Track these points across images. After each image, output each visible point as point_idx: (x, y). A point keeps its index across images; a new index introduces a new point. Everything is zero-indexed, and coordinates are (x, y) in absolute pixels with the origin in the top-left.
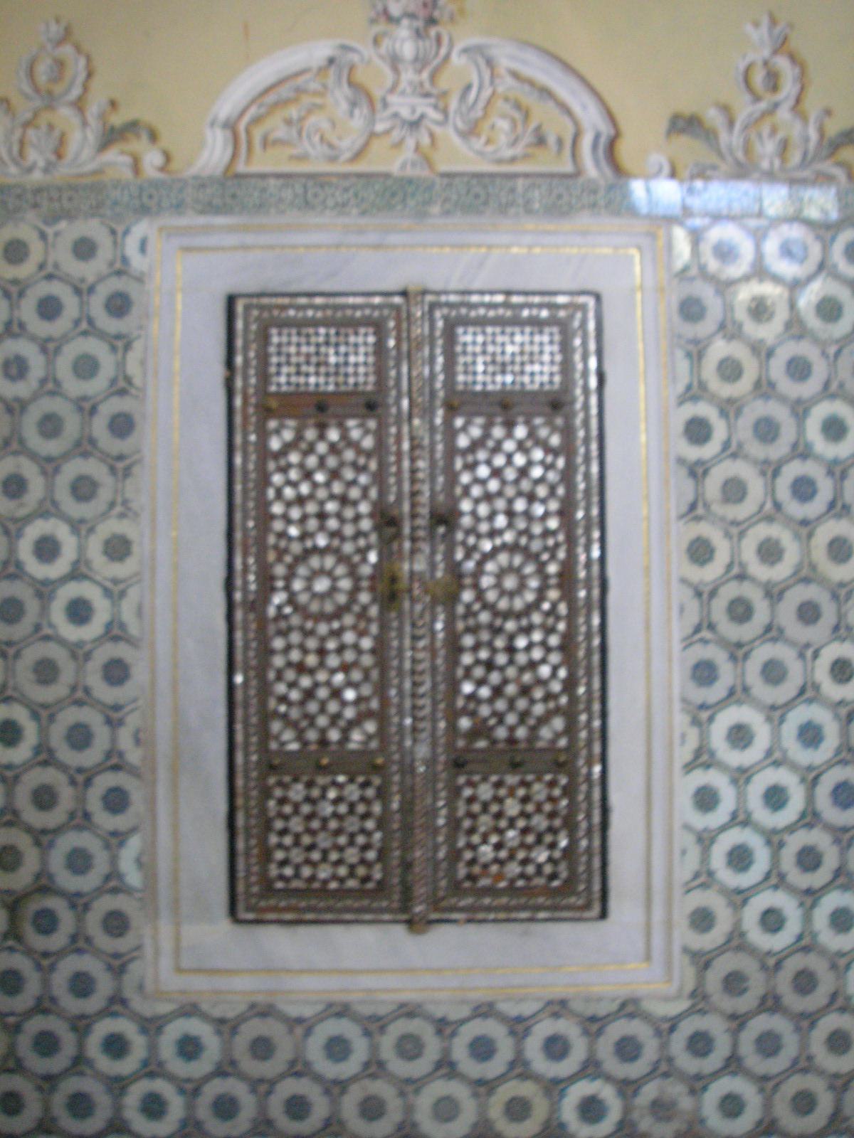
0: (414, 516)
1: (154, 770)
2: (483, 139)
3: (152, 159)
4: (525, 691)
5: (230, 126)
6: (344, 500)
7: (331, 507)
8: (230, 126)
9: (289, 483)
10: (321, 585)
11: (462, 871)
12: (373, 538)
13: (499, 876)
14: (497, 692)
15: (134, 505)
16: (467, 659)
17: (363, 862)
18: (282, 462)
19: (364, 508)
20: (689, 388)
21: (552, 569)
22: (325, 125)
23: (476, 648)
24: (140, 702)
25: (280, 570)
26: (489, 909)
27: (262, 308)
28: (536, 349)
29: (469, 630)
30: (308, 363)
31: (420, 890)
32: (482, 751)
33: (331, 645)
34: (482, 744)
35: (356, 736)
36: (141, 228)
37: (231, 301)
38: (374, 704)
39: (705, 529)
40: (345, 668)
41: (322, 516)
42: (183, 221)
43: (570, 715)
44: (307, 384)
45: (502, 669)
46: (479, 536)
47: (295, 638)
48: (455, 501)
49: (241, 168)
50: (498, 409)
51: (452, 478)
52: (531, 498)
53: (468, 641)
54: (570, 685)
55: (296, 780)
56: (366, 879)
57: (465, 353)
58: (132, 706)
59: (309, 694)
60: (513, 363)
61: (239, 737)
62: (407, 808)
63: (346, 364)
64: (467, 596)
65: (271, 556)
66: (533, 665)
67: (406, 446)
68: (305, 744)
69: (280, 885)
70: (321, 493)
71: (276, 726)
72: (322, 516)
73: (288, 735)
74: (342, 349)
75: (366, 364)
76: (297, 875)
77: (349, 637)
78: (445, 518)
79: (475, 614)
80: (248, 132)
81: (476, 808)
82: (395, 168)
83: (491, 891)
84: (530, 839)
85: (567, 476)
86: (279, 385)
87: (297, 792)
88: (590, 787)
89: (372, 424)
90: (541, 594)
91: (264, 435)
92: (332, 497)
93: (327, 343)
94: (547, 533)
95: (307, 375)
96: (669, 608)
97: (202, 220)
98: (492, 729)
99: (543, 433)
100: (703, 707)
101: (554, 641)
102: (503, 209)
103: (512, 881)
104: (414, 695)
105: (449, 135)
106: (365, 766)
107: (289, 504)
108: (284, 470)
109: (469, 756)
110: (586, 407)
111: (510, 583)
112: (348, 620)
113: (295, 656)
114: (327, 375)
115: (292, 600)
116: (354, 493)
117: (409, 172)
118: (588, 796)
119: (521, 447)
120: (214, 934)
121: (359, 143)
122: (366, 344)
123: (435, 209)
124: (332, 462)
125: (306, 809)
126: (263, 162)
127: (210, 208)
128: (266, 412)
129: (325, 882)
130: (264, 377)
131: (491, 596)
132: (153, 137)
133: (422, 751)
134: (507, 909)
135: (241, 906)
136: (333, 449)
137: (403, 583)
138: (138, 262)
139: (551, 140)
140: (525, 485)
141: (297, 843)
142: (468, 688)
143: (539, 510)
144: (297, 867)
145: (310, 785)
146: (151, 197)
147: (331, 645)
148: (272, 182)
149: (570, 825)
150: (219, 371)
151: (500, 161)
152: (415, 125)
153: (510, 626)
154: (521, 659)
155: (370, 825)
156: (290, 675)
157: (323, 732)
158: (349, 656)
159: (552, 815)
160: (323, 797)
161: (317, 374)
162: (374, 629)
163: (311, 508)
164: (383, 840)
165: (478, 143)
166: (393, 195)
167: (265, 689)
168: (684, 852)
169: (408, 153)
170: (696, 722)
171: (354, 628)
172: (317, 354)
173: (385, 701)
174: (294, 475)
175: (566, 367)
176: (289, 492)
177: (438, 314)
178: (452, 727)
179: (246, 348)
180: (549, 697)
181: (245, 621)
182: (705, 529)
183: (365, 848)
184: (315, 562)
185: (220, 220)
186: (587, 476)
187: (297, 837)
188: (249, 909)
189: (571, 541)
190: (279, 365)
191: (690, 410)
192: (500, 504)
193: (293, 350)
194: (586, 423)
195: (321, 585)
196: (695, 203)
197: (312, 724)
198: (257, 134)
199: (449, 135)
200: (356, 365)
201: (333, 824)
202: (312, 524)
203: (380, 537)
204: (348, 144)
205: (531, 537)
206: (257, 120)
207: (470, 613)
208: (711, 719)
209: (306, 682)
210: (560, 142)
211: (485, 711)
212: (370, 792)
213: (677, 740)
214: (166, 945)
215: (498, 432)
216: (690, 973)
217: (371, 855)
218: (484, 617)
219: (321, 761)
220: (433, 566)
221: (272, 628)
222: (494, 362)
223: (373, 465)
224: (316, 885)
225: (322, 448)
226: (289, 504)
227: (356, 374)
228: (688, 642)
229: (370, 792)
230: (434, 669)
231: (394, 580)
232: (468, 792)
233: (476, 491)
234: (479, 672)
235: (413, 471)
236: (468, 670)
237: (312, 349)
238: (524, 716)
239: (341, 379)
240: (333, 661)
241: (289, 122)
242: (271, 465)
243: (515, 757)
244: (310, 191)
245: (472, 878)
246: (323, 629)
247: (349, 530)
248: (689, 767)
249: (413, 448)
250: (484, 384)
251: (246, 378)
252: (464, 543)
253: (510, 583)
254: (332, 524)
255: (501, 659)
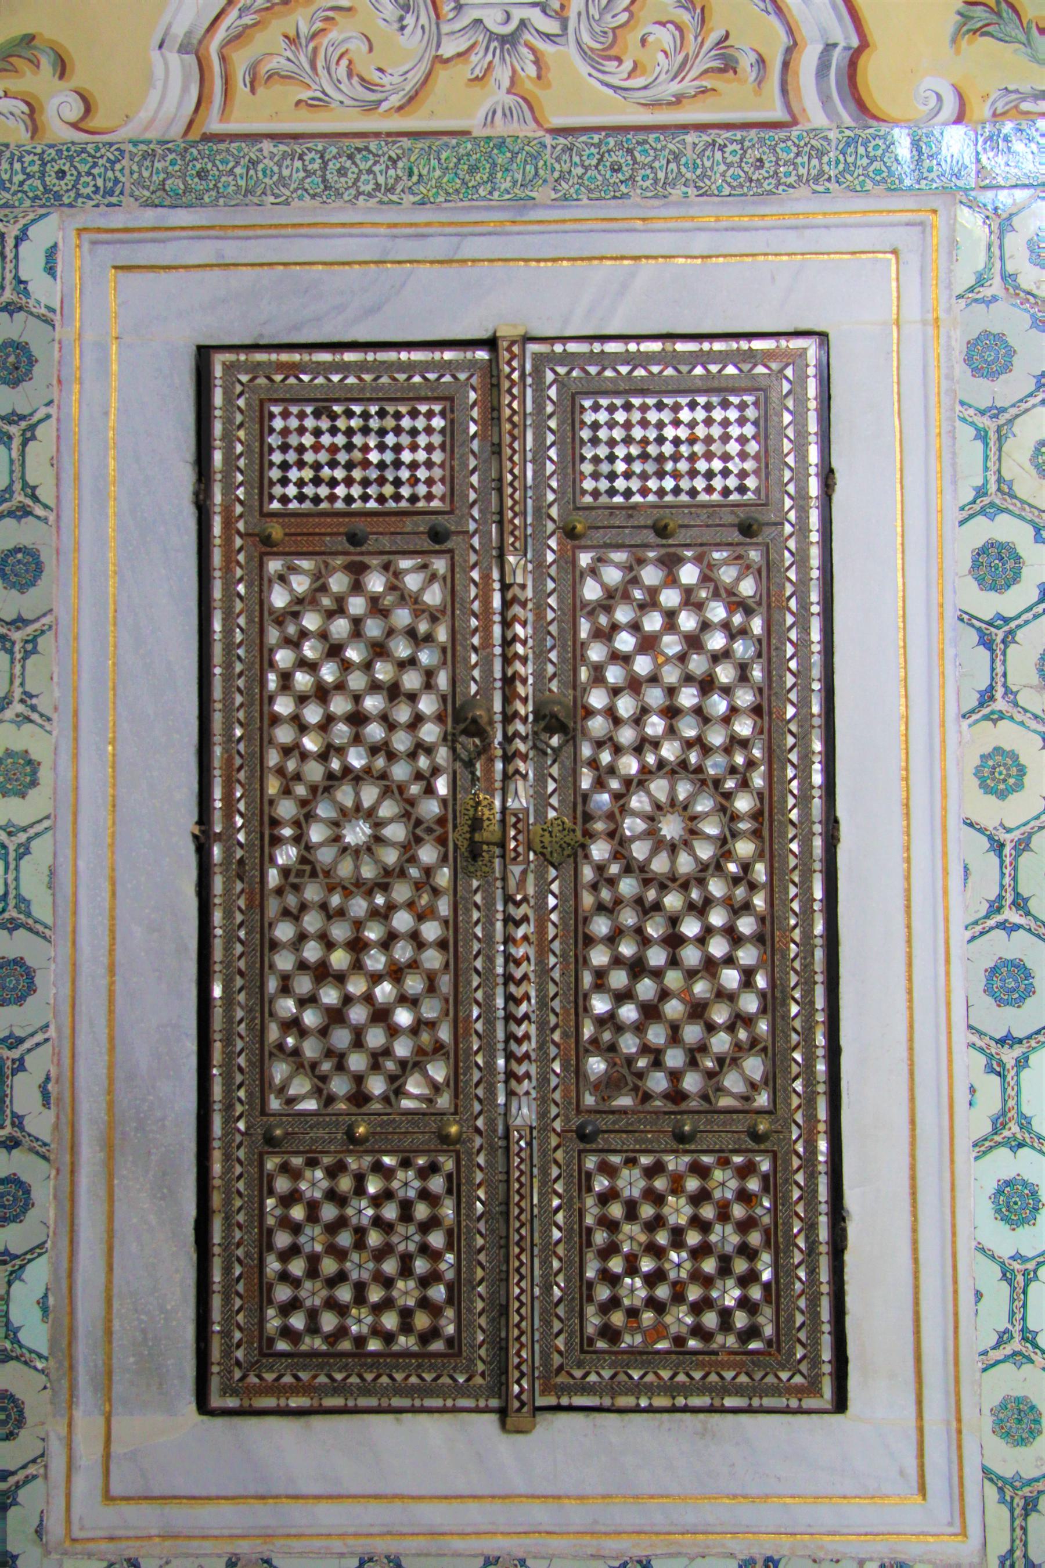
0: (508, 718)
1: (74, 1148)
2: (628, 65)
3: (61, 107)
4: (698, 1011)
5: (194, 49)
6: (394, 692)
7: (372, 703)
8: (194, 49)
9: (303, 664)
10: (357, 834)
11: (593, 1321)
12: (442, 755)
13: (659, 1331)
14: (651, 1012)
15: (43, 704)
16: (599, 957)
17: (424, 1303)
18: (291, 630)
19: (427, 705)
20: (981, 492)
21: (743, 804)
22: (358, 47)
23: (612, 939)
24: (52, 1032)
25: (286, 809)
26: (638, 1389)
27: (255, 368)
28: (716, 431)
29: (601, 908)
30: (333, 464)
31: (520, 1354)
32: (623, 1111)
33: (372, 934)
34: (625, 1101)
35: (414, 1086)
36: (48, 230)
37: (204, 354)
38: (444, 1034)
39: (1008, 735)
40: (396, 973)
41: (357, 719)
42: (117, 219)
43: (775, 1055)
44: (332, 498)
45: (657, 974)
46: (618, 750)
47: (312, 922)
48: (579, 690)
49: (215, 126)
50: (651, 537)
51: (576, 653)
52: (707, 685)
53: (601, 926)
54: (773, 1002)
55: (312, 1163)
56: (433, 1333)
57: (595, 441)
58: (39, 1038)
59: (336, 1016)
60: (676, 457)
61: (217, 1091)
62: (502, 1211)
63: (398, 464)
64: (599, 851)
65: (273, 786)
66: (710, 966)
67: (497, 602)
68: (330, 1100)
69: (282, 1346)
70: (356, 681)
71: (279, 1071)
72: (357, 719)
73: (300, 1086)
74: (390, 440)
75: (429, 464)
76: (313, 1328)
77: (402, 921)
78: (560, 721)
79: (612, 882)
80: (223, 59)
81: (616, 1211)
82: (474, 123)
83: (644, 1356)
84: (709, 1266)
85: (768, 648)
86: (284, 500)
87: (315, 1182)
88: (812, 1177)
89: (440, 565)
90: (723, 845)
91: (261, 584)
92: (375, 687)
93: (366, 431)
94: (737, 743)
95: (333, 483)
96: (945, 872)
97: (150, 217)
98: (640, 1075)
99: (727, 575)
100: (1007, 1040)
101: (746, 925)
102: (660, 190)
103: (679, 1341)
104: (509, 1017)
105: (567, 60)
106: (430, 1140)
107: (302, 699)
108: (294, 643)
109: (604, 1122)
110: (802, 529)
111: (671, 828)
112: (401, 892)
113: (312, 952)
114: (365, 483)
115: (307, 863)
116: (411, 681)
117: (500, 128)
118: (809, 1194)
119: (690, 600)
120: (168, 1434)
121: (416, 77)
122: (429, 430)
123: (543, 194)
124: (373, 629)
125: (329, 1212)
126: (251, 113)
127: (163, 197)
128: (266, 545)
129: (360, 1341)
130: (262, 488)
131: (639, 851)
132: (62, 67)
133: (525, 1113)
134: (671, 1389)
135: (215, 1383)
136: (376, 607)
137: (491, 831)
138: (43, 291)
139: (746, 62)
140: (697, 664)
141: (313, 1272)
142: (600, 1005)
143: (719, 705)
144: (313, 1316)
145: (334, 1172)
146: (61, 174)
147: (372, 934)
148: (267, 146)
149: (777, 1241)
150: (186, 475)
151: (655, 104)
152: (509, 41)
153: (673, 901)
154: (691, 956)
155: (436, 1239)
156: (303, 985)
157: (359, 1079)
158: (403, 952)
159: (745, 1226)
160: (360, 1190)
161: (349, 482)
162: (444, 907)
163: (340, 705)
164: (458, 1266)
165: (618, 73)
166: (473, 170)
167: (262, 1008)
168: (979, 1295)
169: (497, 95)
170: (996, 1068)
171: (410, 905)
172: (349, 447)
173: (460, 1028)
174: (310, 650)
175: (767, 462)
176: (302, 680)
177: (550, 376)
178: (578, 1071)
179: (229, 438)
180: (740, 1020)
181: (227, 891)
182: (1008, 735)
183: (431, 1278)
184: (345, 795)
185: (182, 217)
186: (802, 646)
187: (313, 1260)
188: (227, 1390)
189: (774, 758)
190: (285, 466)
191: (982, 531)
192: (655, 697)
193: (308, 440)
194: (801, 560)
195: (357, 834)
196: (995, 163)
197: (341, 1066)
198: (241, 61)
199: (567, 60)
200: (414, 466)
201: (374, 1239)
202: (342, 731)
203: (455, 756)
204: (396, 81)
205: (706, 750)
206: (238, 38)
207: (603, 879)
208: (1022, 1063)
209: (330, 996)
210: (761, 61)
211: (629, 1044)
212: (437, 1184)
213: (961, 1096)
214: (88, 1453)
215: (651, 575)
216: (999, 1516)
217: (438, 1293)
218: (628, 887)
219: (356, 1129)
220: (541, 799)
221: (273, 907)
222: (644, 456)
223: (442, 635)
224: (346, 1345)
225: (357, 605)
226: (302, 699)
227: (414, 481)
228: (978, 931)
229: (437, 1184)
230: (544, 971)
231: (476, 824)
232: (600, 1184)
233: (614, 675)
234: (619, 979)
235: (507, 643)
236: (600, 974)
237: (340, 440)
238: (694, 1054)
239: (388, 490)
240: (375, 961)
241: (292, 40)
242: (273, 635)
243: (680, 1121)
244: (331, 163)
245: (610, 1333)
246: (359, 906)
247: (401, 742)
248: (983, 1147)
249: (506, 604)
250: (628, 493)
251: (229, 488)
252: (593, 763)
253: (671, 828)
254: (375, 731)
255: (656, 957)
